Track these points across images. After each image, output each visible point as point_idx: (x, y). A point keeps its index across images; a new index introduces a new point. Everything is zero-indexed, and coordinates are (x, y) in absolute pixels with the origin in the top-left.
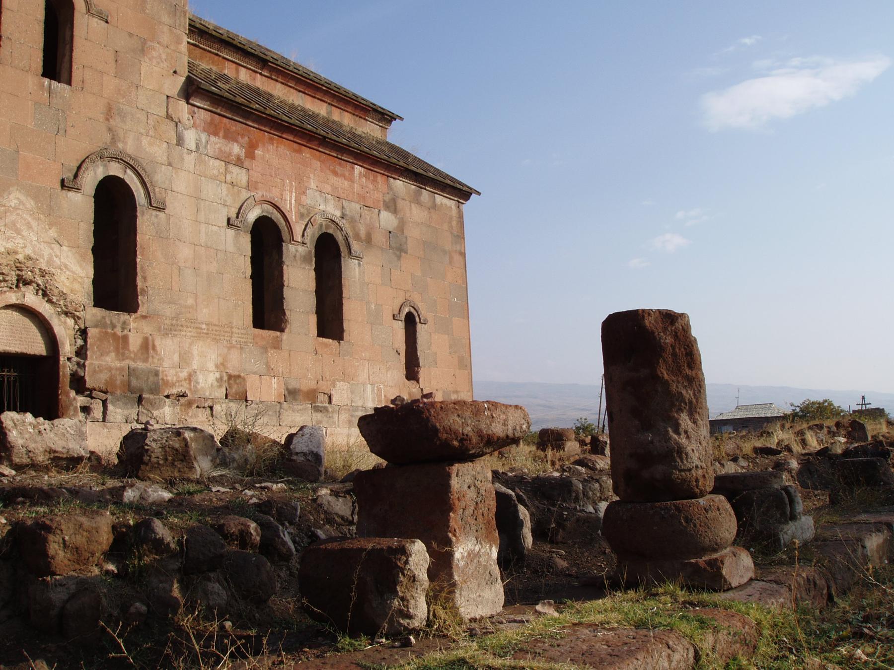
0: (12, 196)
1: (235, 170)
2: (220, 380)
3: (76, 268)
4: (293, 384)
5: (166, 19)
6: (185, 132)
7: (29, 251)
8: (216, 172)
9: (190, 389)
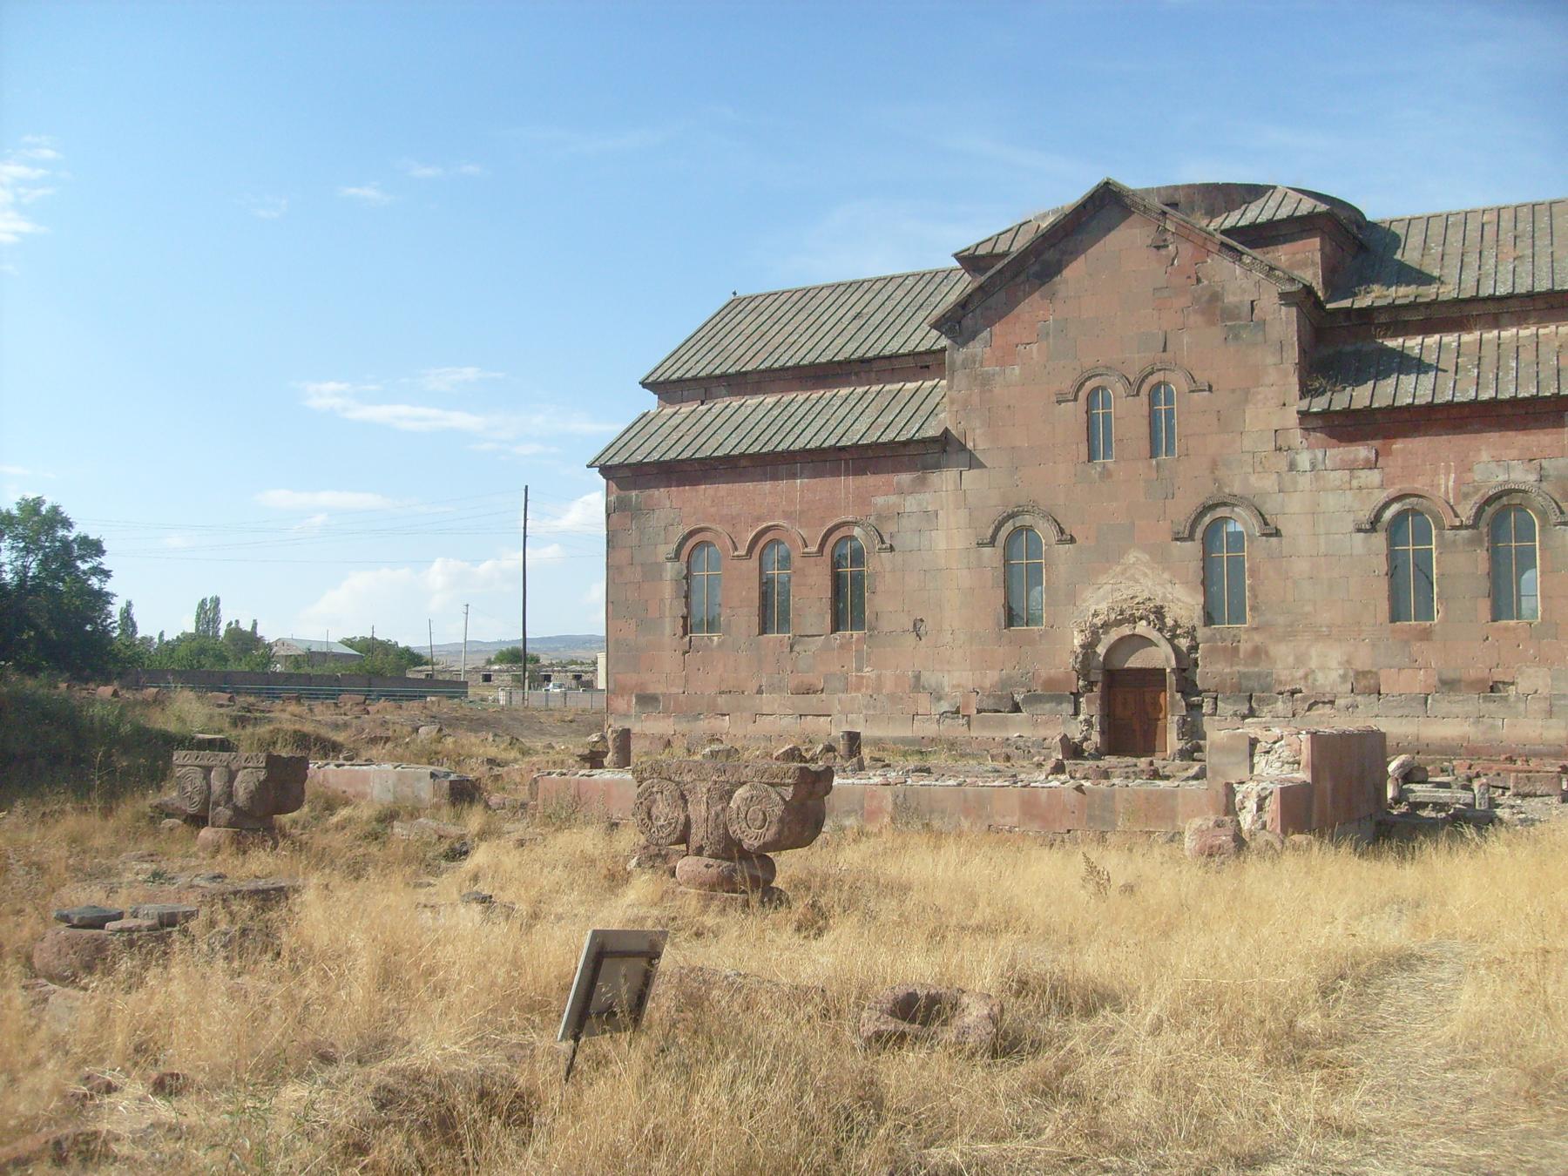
0: (1131, 556)
1: (1363, 474)
2: (1344, 677)
3: (1189, 600)
4: (1450, 674)
5: (1271, 360)
6: (1298, 457)
7: (1146, 595)
8: (1338, 483)
9: (1307, 687)
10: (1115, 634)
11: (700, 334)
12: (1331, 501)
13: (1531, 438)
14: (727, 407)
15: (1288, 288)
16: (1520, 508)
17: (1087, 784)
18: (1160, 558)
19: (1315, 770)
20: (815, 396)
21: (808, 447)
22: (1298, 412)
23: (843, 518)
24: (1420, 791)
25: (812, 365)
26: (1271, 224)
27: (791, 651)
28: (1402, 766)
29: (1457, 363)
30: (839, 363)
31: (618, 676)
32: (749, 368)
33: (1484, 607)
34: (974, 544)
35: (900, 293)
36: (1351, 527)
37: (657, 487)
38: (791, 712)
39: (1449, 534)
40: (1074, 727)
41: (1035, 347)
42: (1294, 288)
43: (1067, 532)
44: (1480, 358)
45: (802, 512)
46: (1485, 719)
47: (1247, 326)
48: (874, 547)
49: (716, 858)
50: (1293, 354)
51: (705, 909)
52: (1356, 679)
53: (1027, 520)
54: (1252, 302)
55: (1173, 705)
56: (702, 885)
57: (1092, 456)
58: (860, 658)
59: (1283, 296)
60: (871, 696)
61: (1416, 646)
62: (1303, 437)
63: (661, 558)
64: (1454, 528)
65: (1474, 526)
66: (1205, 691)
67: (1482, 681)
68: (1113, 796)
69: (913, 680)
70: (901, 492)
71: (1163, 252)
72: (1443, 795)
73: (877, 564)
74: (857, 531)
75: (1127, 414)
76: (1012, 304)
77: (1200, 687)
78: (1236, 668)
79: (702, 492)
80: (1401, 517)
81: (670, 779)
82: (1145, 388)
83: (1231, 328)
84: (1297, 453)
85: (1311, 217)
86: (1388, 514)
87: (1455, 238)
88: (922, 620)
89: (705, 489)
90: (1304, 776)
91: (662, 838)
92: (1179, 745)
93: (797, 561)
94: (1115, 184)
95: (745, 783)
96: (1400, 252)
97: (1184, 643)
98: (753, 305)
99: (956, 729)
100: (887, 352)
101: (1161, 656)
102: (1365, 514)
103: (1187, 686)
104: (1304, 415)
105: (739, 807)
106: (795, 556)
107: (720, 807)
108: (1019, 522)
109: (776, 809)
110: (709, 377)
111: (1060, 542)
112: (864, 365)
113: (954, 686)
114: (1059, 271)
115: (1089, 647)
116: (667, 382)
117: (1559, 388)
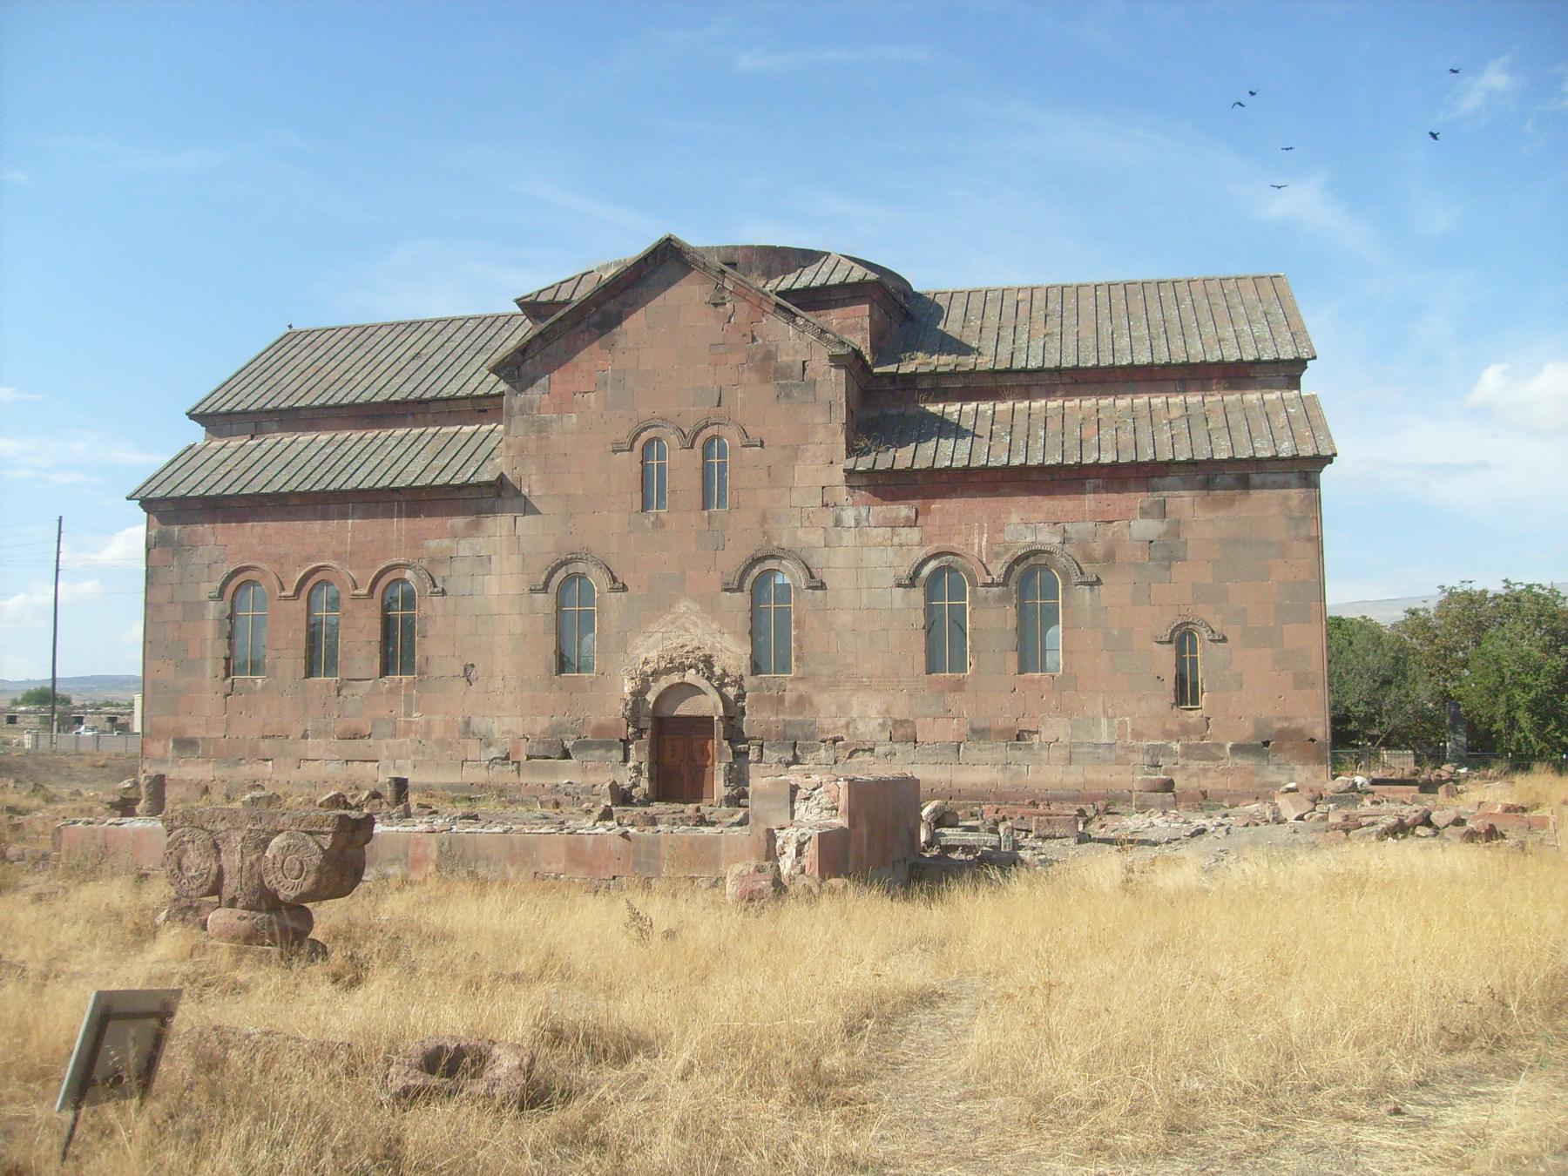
1: (904, 531)
2: (883, 726)
4: (982, 724)
5: (819, 419)
6: (843, 513)
7: (695, 644)
10: (664, 682)
11: (253, 367)
12: (874, 557)
13: (1057, 502)
14: (278, 443)
15: (838, 351)
16: (1045, 568)
17: (632, 830)
18: (710, 607)
19: (852, 815)
20: (370, 435)
21: (360, 487)
22: (845, 470)
23: (395, 561)
24: (951, 835)
25: (368, 404)
26: (824, 288)
27: (338, 695)
28: (934, 811)
29: (992, 430)
30: (396, 402)
31: (155, 719)
32: (302, 403)
33: (1012, 660)
34: (527, 590)
35: (460, 335)
36: (891, 582)
37: (202, 523)
38: (337, 757)
39: (982, 591)
40: (623, 773)
41: (592, 396)
42: (844, 352)
43: (620, 580)
44: (1012, 427)
45: (352, 553)
46: (1012, 766)
47: (798, 385)
48: (426, 591)
49: (251, 910)
50: (841, 415)
51: (237, 964)
52: (894, 728)
53: (580, 567)
54: (804, 362)
55: (720, 753)
56: (235, 938)
57: (645, 507)
58: (409, 703)
59: (833, 358)
60: (420, 742)
61: (950, 698)
62: (848, 494)
63: (204, 597)
64: (986, 585)
65: (1004, 584)
66: (751, 739)
67: (1009, 730)
68: (659, 845)
69: (463, 725)
70: (454, 535)
71: (720, 309)
72: (971, 838)
73: (428, 606)
74: (408, 574)
75: (682, 466)
76: (572, 352)
77: (746, 735)
78: (781, 717)
79: (248, 529)
80: (938, 572)
81: (202, 828)
82: (699, 441)
83: (782, 386)
84: (842, 510)
85: (862, 284)
86: (926, 571)
87: (993, 312)
88: (472, 666)
89: (252, 527)
90: (841, 821)
91: (193, 889)
92: (726, 792)
93: (346, 604)
94: (677, 240)
95: (281, 831)
96: (942, 322)
97: (731, 692)
98: (309, 339)
99: (506, 775)
100: (444, 394)
101: (709, 704)
102: (905, 571)
103: (735, 734)
104: (850, 473)
105: (275, 857)
106: (344, 597)
107: (254, 857)
108: (572, 569)
109: (314, 858)
110: (260, 411)
111: (613, 590)
112: (421, 406)
113: (503, 733)
114: (619, 323)
115: (639, 694)
116: (216, 414)
117: (1081, 458)
